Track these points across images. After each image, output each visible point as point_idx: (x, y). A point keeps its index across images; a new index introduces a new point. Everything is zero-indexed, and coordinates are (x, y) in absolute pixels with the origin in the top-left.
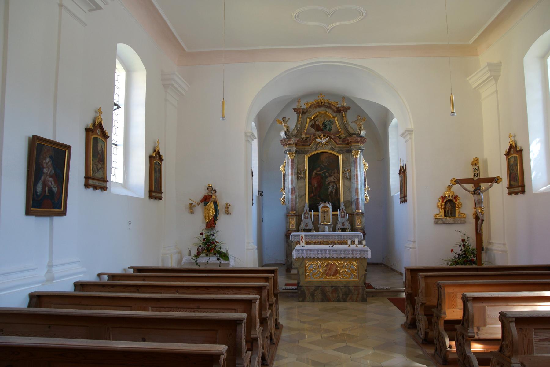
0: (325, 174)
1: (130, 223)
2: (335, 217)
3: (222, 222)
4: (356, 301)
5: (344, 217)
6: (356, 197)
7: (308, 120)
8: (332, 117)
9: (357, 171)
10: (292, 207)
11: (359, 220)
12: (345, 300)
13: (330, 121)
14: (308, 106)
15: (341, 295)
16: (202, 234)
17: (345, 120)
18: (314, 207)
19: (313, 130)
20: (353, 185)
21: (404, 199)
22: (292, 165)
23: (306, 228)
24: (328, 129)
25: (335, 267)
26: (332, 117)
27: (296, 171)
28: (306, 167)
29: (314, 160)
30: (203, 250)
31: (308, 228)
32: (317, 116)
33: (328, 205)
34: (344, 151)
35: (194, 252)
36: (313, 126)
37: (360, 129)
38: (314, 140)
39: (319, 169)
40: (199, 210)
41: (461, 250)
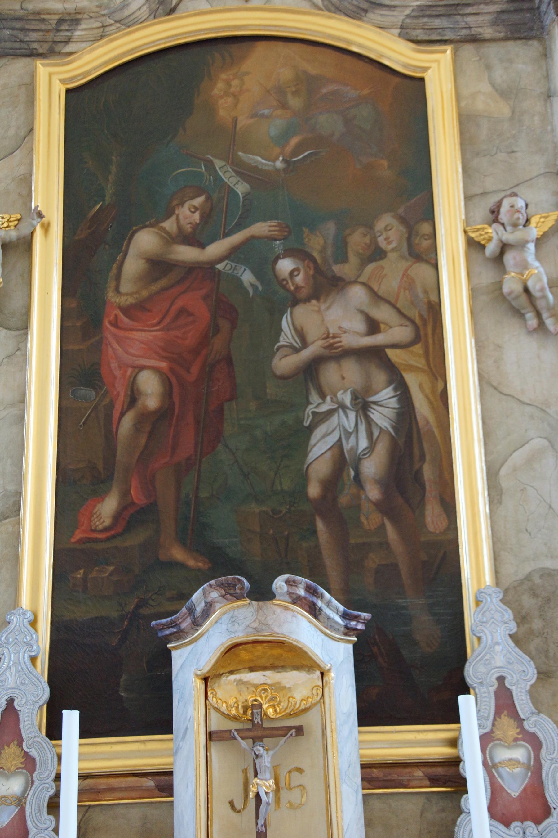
28: (49, 193)
39: (188, 214)
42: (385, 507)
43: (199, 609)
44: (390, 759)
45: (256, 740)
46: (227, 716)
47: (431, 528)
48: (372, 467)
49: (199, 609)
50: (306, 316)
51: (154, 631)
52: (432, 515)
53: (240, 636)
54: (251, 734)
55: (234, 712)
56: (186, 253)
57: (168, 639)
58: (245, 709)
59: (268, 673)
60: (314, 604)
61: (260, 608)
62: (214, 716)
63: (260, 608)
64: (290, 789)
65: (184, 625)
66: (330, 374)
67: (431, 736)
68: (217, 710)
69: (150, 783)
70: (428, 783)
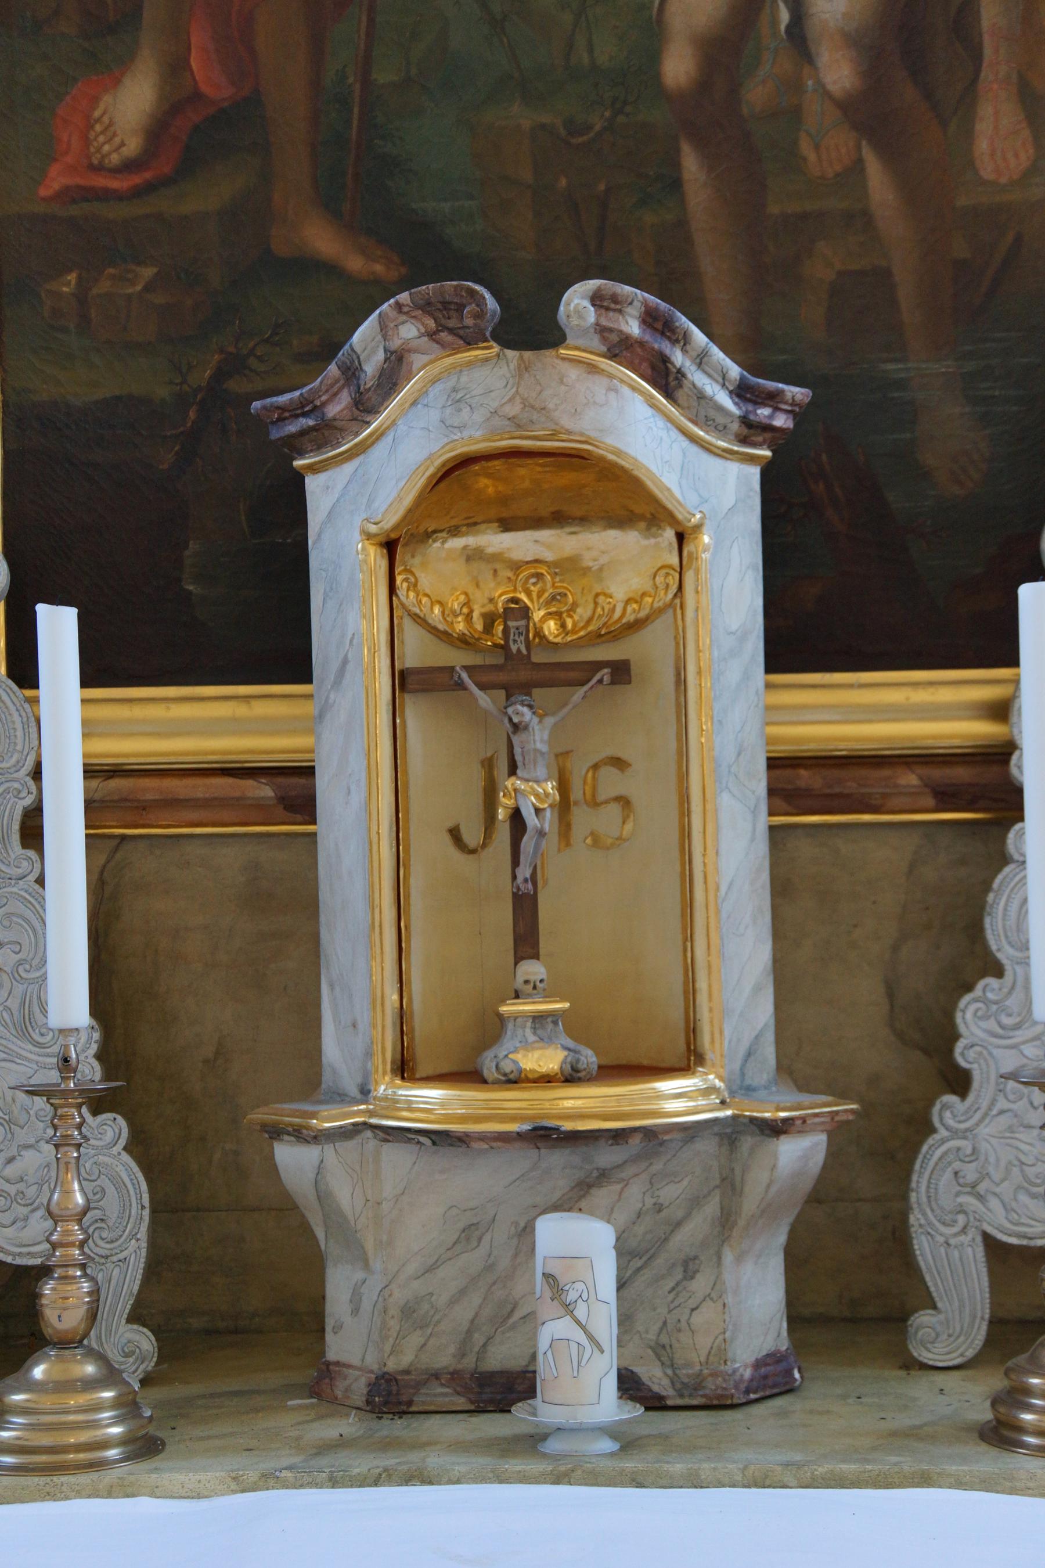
33: (636, 428)
42: (869, 115)
43: (372, 366)
44: (842, 748)
45: (512, 691)
46: (444, 636)
47: (987, 172)
49: (372, 366)
51: (261, 424)
53: (474, 438)
54: (502, 677)
55: (460, 626)
57: (295, 445)
58: (489, 620)
59: (545, 535)
60: (665, 360)
61: (524, 368)
62: (411, 635)
63: (524, 368)
64: (595, 804)
65: (333, 410)
67: (946, 695)
68: (420, 620)
69: (263, 791)
70: (930, 802)
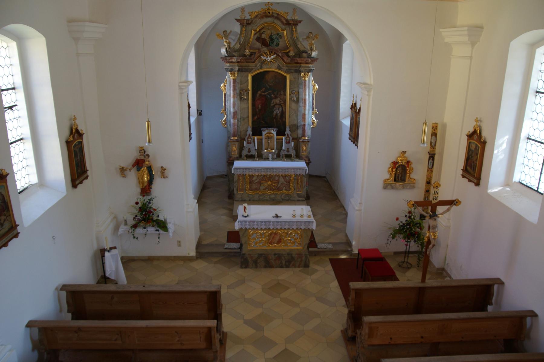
0: (270, 95)
1: (54, 238)
2: (280, 142)
3: (158, 185)
4: (299, 267)
5: (289, 143)
6: (303, 123)
7: (253, 31)
8: (280, 30)
9: (305, 95)
10: (234, 132)
11: (304, 148)
12: (287, 266)
13: (278, 34)
14: (253, 16)
15: (284, 262)
16: (137, 203)
17: (295, 36)
18: (257, 131)
19: (258, 44)
20: (300, 109)
21: (354, 138)
22: (234, 86)
23: (248, 154)
24: (275, 43)
25: (279, 236)
26: (280, 30)
27: (238, 91)
28: (250, 87)
29: (259, 80)
30: (140, 221)
31: (251, 154)
32: (263, 28)
33: (272, 132)
34: (292, 71)
35: (131, 222)
36: (258, 39)
37: (312, 50)
38: (259, 56)
39: (263, 90)
40: (132, 175)
41: (406, 221)
48: (279, 115)
50: (274, 100)
52: (284, 119)
56: (263, 94)
66: (276, 106)
